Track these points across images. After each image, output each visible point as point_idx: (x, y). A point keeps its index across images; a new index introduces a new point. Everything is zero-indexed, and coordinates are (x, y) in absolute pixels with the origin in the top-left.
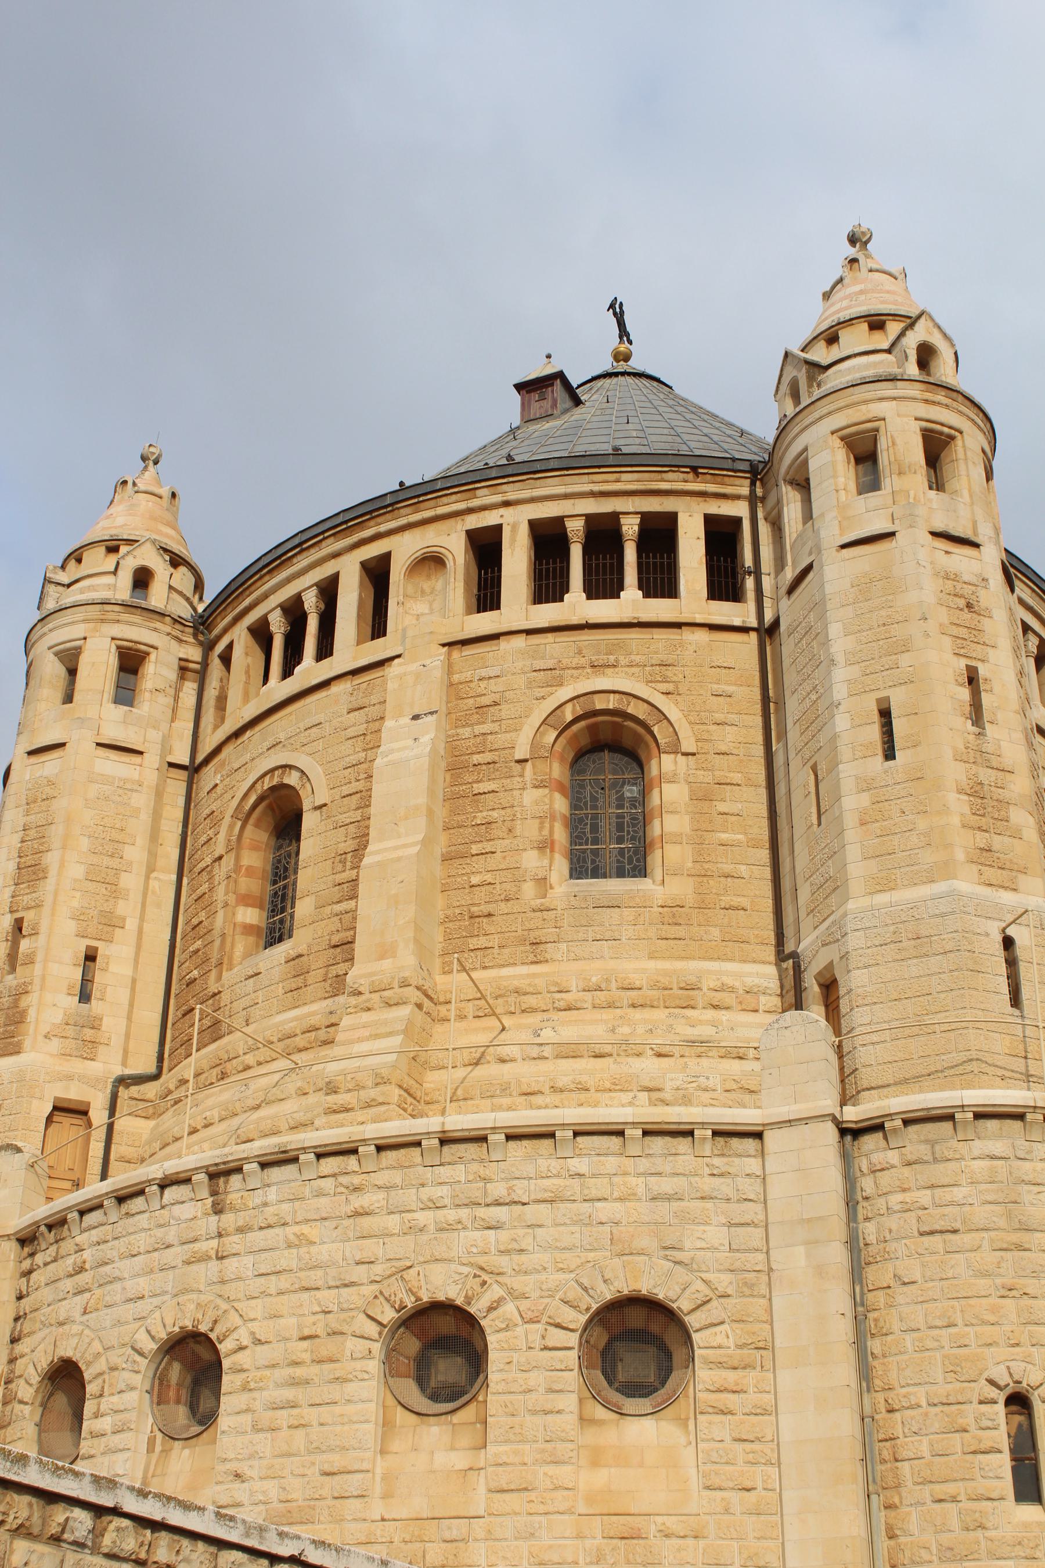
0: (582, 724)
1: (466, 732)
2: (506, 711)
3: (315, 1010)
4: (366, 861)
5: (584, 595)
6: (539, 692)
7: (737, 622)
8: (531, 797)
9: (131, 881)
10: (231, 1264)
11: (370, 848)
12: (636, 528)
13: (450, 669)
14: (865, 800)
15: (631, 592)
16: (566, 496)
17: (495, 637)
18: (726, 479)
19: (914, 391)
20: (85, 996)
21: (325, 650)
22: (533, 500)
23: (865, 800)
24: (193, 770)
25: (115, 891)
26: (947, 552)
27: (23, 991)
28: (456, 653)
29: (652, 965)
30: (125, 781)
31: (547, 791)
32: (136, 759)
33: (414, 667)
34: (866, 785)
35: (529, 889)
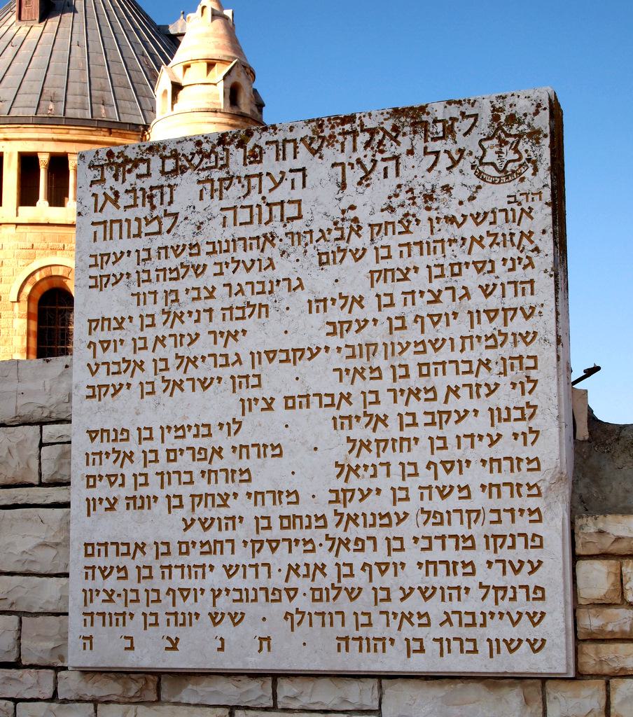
0: (45, 282)
5: (47, 203)
6: (21, 263)
16: (39, 140)
18: (127, 136)
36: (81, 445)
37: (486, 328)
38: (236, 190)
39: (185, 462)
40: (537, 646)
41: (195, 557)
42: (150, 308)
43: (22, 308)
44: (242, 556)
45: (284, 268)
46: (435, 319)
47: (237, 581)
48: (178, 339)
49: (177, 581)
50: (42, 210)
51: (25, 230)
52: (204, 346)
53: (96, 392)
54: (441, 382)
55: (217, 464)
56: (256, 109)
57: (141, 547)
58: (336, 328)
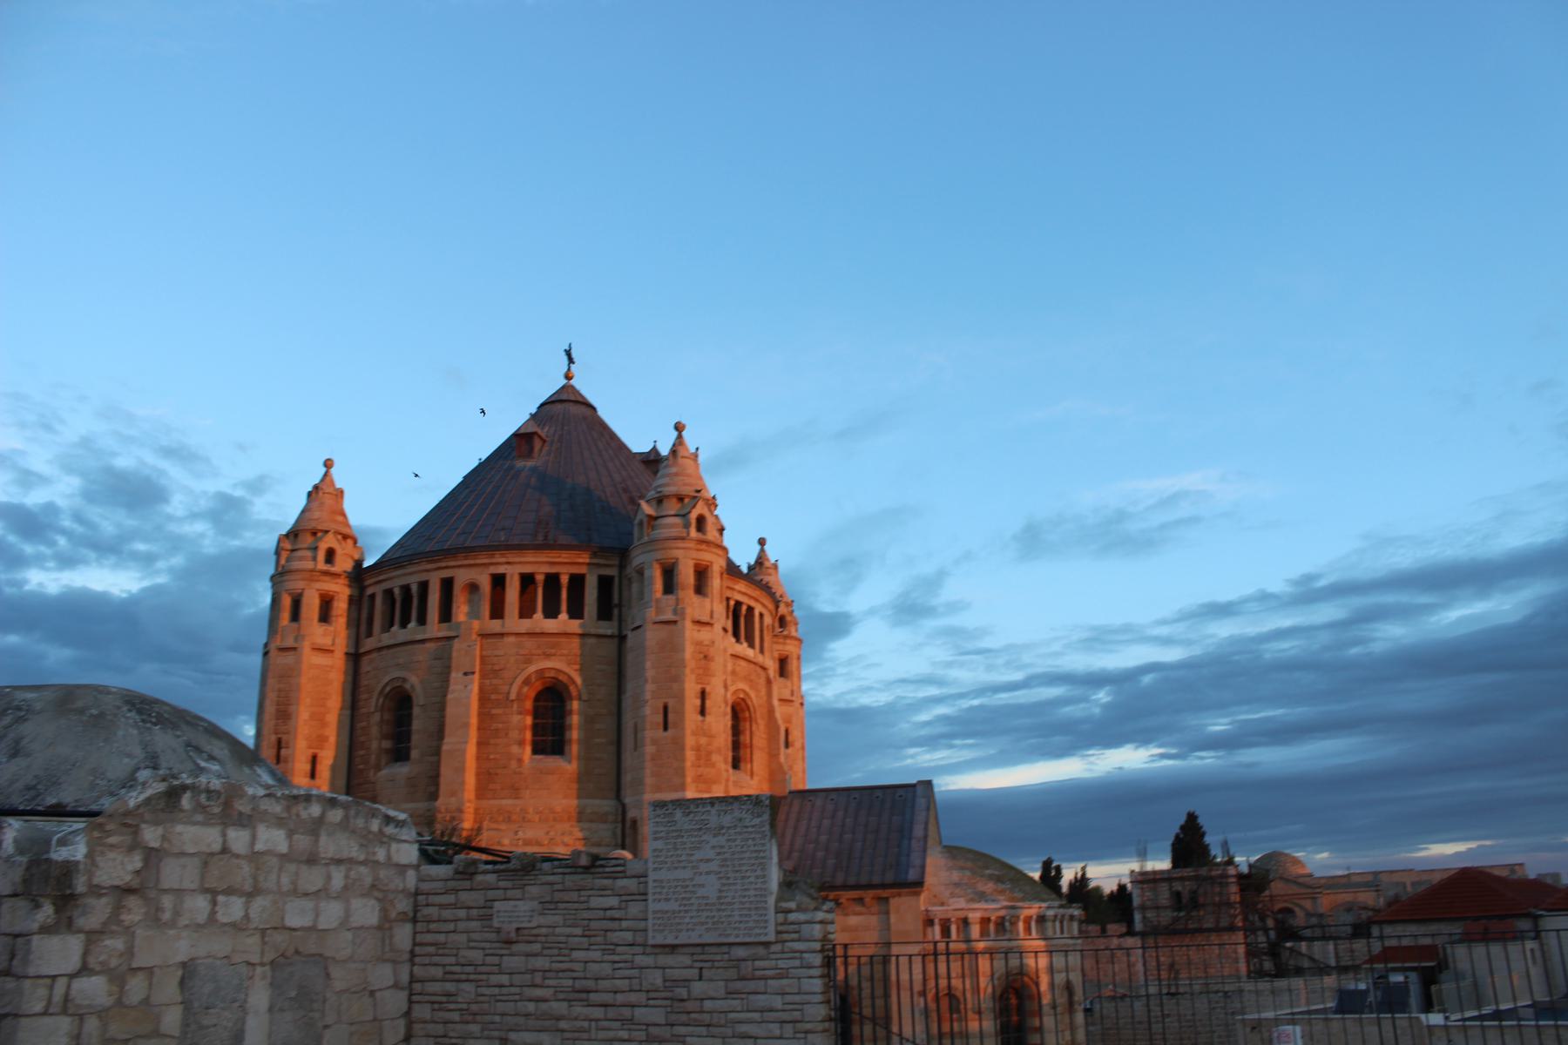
1: (488, 682)
7: (609, 632)
8: (516, 719)
11: (446, 740)
12: (567, 581)
15: (563, 616)
17: (502, 635)
19: (692, 545)
21: (422, 620)
22: (520, 563)
25: (323, 724)
26: (699, 631)
28: (484, 641)
29: (564, 801)
30: (327, 666)
31: (522, 716)
32: (331, 654)
34: (655, 742)
35: (514, 764)
36: (651, 884)
37: (754, 855)
38: (692, 815)
39: (679, 888)
40: (766, 934)
41: (682, 914)
42: (669, 847)
44: (694, 914)
45: (704, 838)
46: (743, 852)
47: (693, 920)
48: (677, 855)
49: (677, 920)
51: (524, 639)
52: (683, 858)
53: (655, 869)
54: (744, 868)
55: (687, 890)
56: (717, 534)
57: (667, 912)
58: (719, 854)
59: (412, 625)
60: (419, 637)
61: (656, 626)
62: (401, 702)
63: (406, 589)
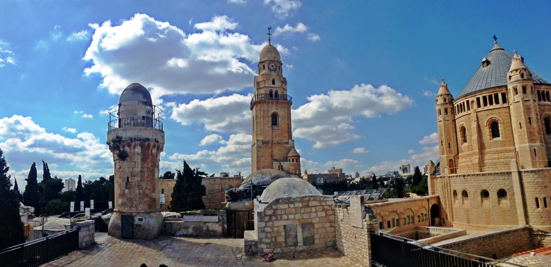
2: (483, 120)
3: (471, 152)
4: (472, 139)
7: (506, 106)
9: (452, 134)
10: (467, 184)
13: (477, 115)
14: (519, 134)
15: (494, 104)
20: (450, 147)
21: (465, 111)
23: (519, 134)
24: (454, 120)
25: (450, 136)
27: (444, 148)
33: (473, 115)
34: (519, 132)
35: (488, 140)
43: (488, 127)
50: (489, 107)
59: (463, 112)
60: (464, 114)
61: (515, 103)
62: (463, 129)
63: (460, 104)
